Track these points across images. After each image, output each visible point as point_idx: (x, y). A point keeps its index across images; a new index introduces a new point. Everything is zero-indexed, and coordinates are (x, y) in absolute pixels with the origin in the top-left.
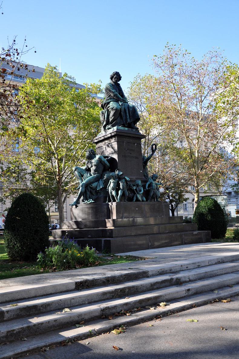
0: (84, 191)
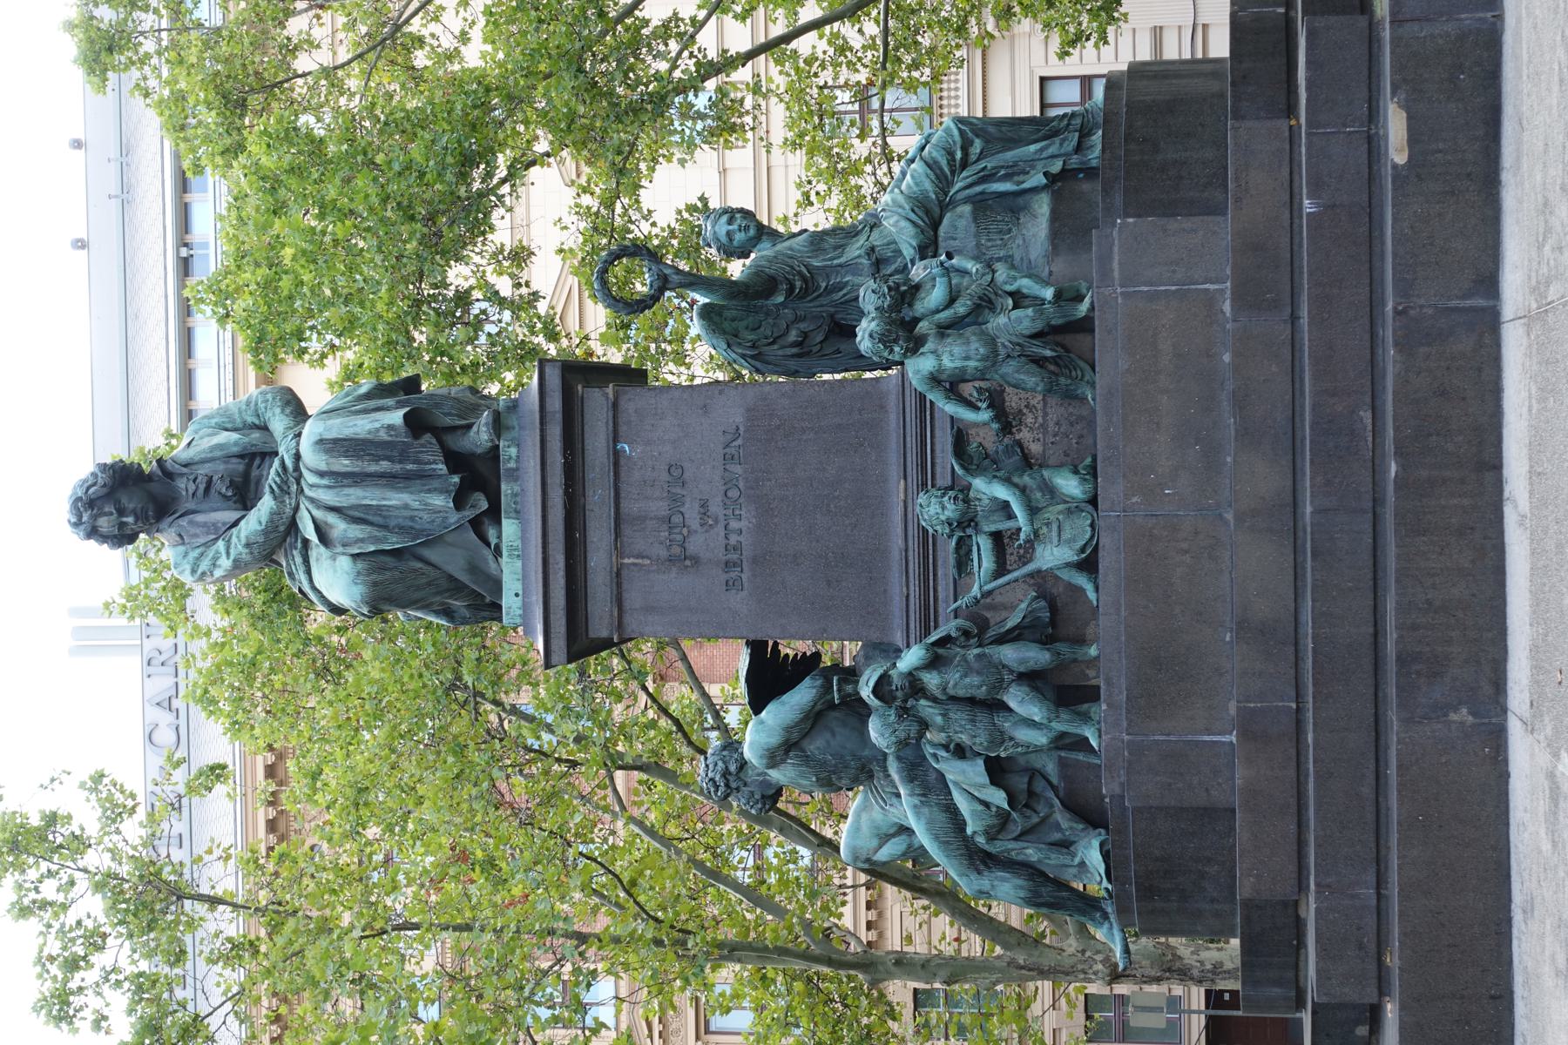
0: (1020, 882)
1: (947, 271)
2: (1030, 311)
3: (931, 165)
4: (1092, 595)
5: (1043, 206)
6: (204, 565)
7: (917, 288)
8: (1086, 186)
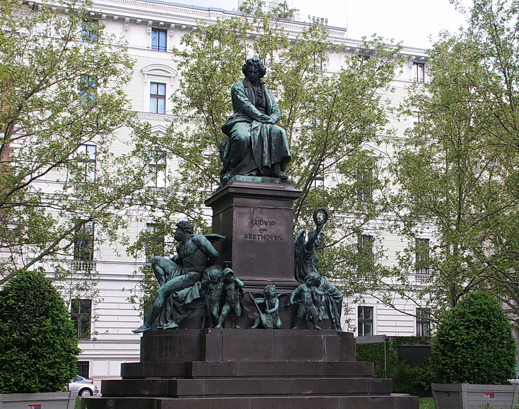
4: (253, 327)
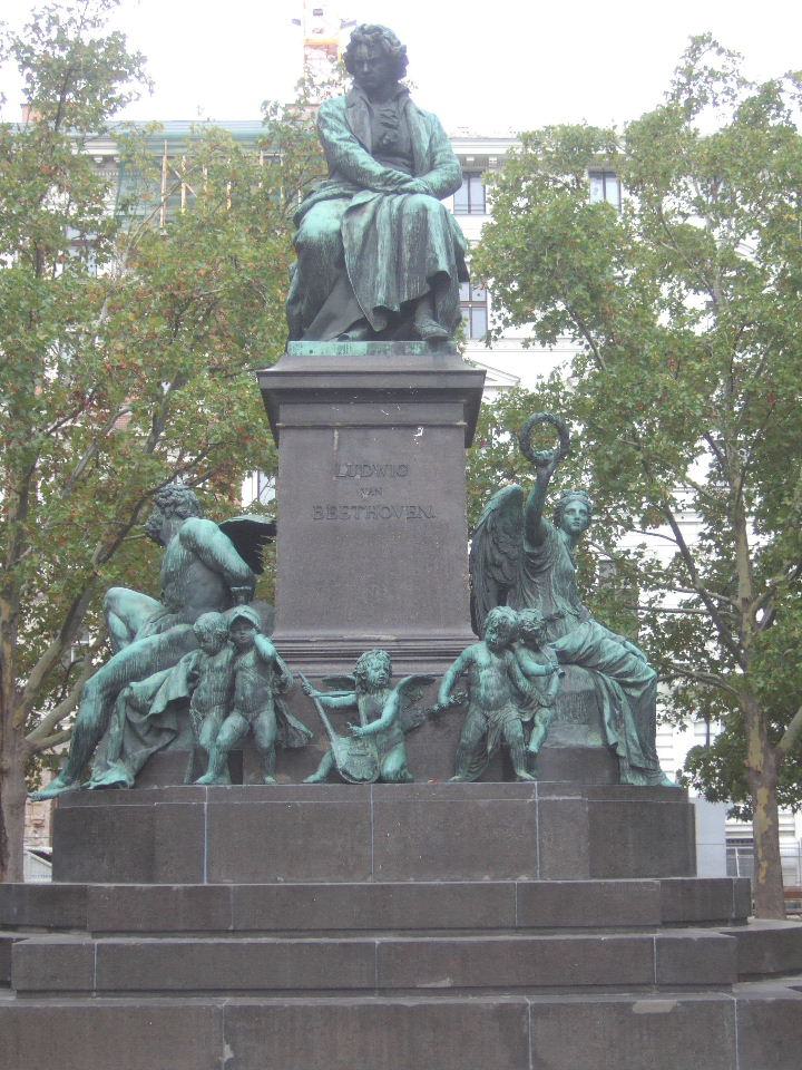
0: (94, 720)
1: (549, 674)
2: (520, 734)
3: (623, 660)
4: (312, 778)
5: (594, 741)
6: (331, 122)
7: (536, 649)
8: (607, 773)
